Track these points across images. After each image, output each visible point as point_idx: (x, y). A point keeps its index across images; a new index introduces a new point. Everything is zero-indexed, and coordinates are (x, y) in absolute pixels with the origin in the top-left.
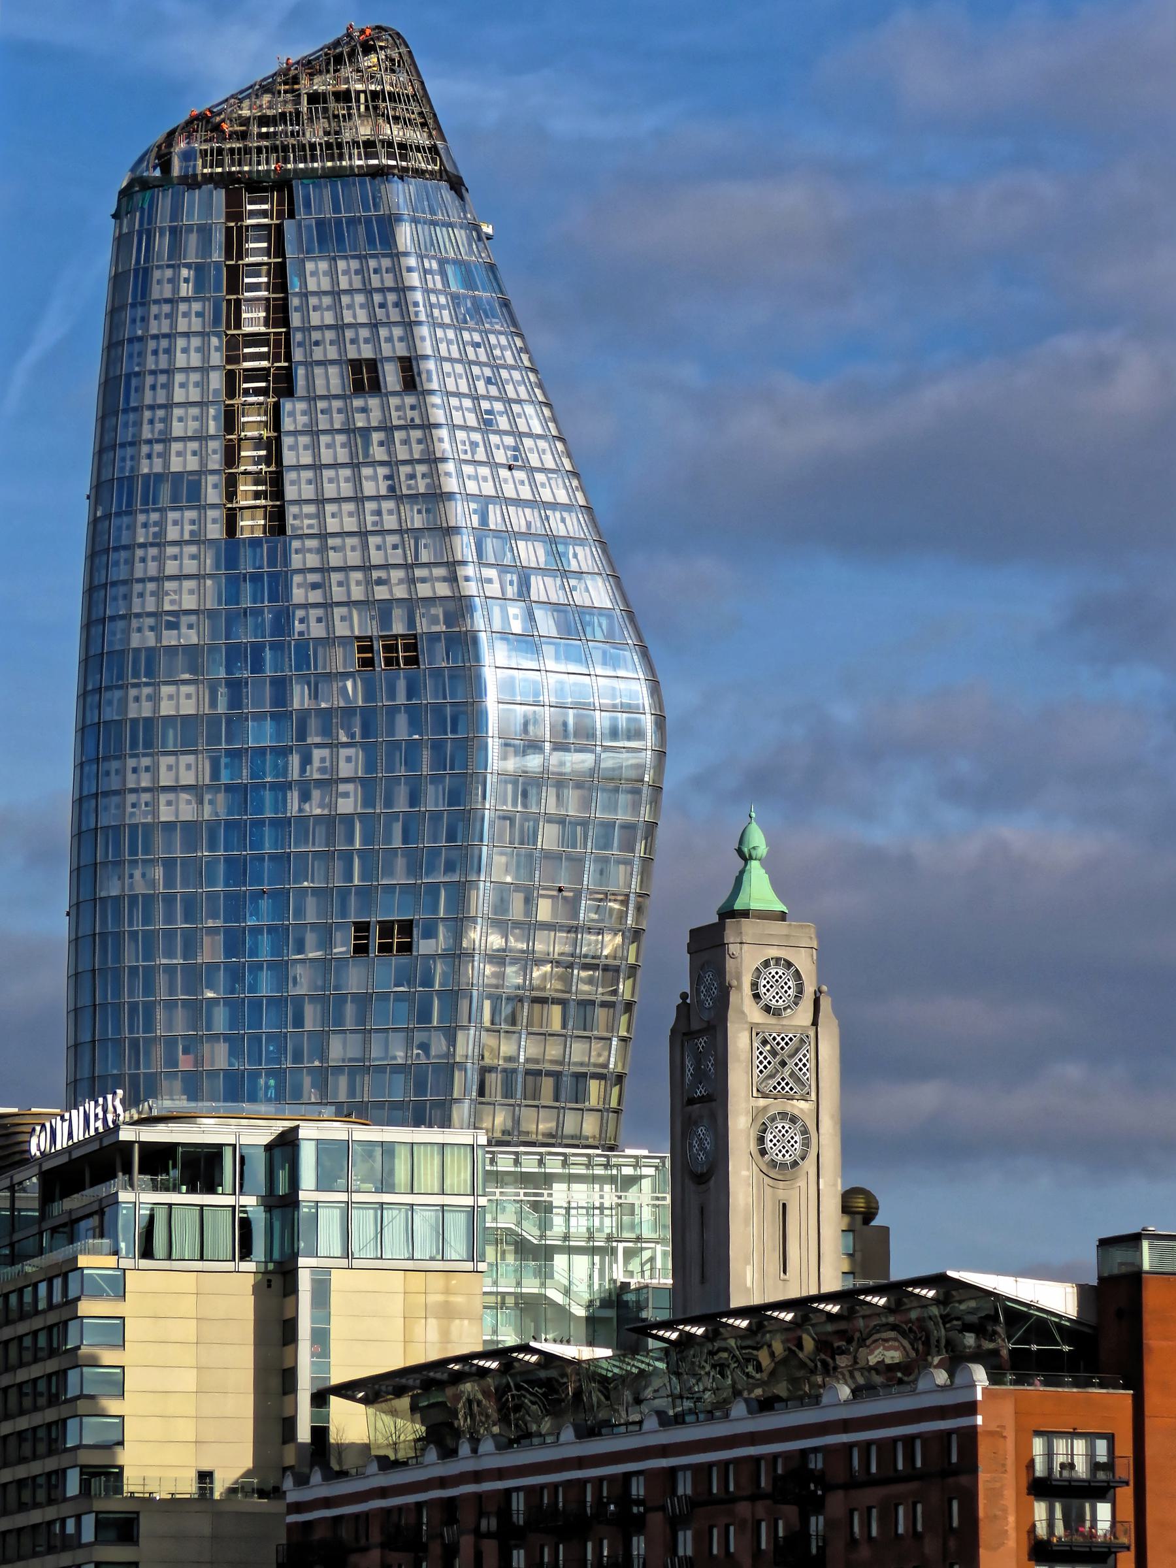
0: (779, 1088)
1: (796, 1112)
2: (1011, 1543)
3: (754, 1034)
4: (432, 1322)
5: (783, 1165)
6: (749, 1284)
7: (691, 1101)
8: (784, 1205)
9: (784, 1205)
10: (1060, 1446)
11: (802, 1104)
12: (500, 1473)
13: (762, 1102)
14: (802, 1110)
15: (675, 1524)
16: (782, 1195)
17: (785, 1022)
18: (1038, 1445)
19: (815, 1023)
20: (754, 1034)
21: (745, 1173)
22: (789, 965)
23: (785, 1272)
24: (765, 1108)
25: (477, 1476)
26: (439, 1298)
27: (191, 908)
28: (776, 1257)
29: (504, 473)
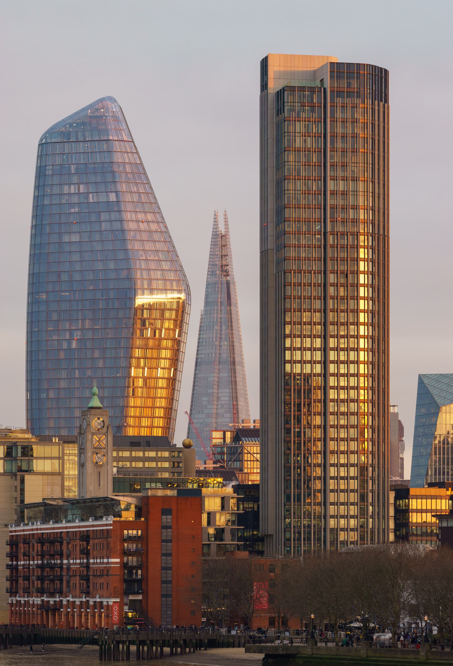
2: (119, 552)
7: (81, 449)
10: (130, 532)
11: (104, 450)
12: (41, 529)
13: (94, 450)
15: (68, 543)
16: (99, 470)
18: (126, 532)
19: (107, 432)
21: (90, 465)
24: (95, 451)
25: (37, 529)
28: (98, 483)
29: (140, 223)
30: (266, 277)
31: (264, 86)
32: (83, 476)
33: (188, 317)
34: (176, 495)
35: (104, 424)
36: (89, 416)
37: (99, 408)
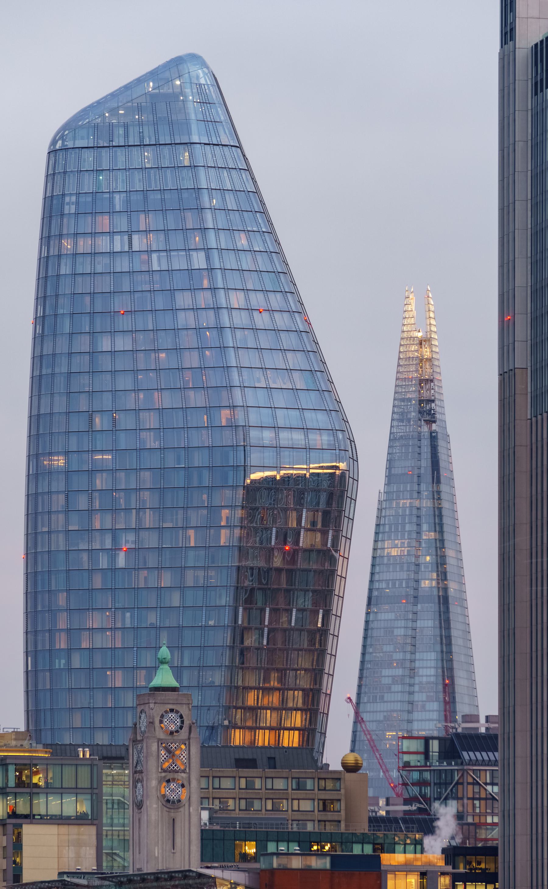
0: (172, 767)
1: (179, 778)
3: (160, 744)
4: (72, 848)
5: (173, 802)
6: (156, 855)
7: (136, 772)
8: (174, 819)
9: (174, 819)
11: (183, 775)
14: (182, 777)
16: (172, 815)
17: (175, 738)
19: (189, 739)
20: (160, 744)
21: (155, 806)
22: (177, 712)
23: (174, 849)
24: (165, 777)
26: (75, 837)
27: (114, 532)
28: (170, 842)
30: (512, 606)
31: (508, 33)
32: (139, 827)
33: (333, 660)
34: (328, 866)
35: (182, 722)
36: (152, 705)
37: (174, 689)
